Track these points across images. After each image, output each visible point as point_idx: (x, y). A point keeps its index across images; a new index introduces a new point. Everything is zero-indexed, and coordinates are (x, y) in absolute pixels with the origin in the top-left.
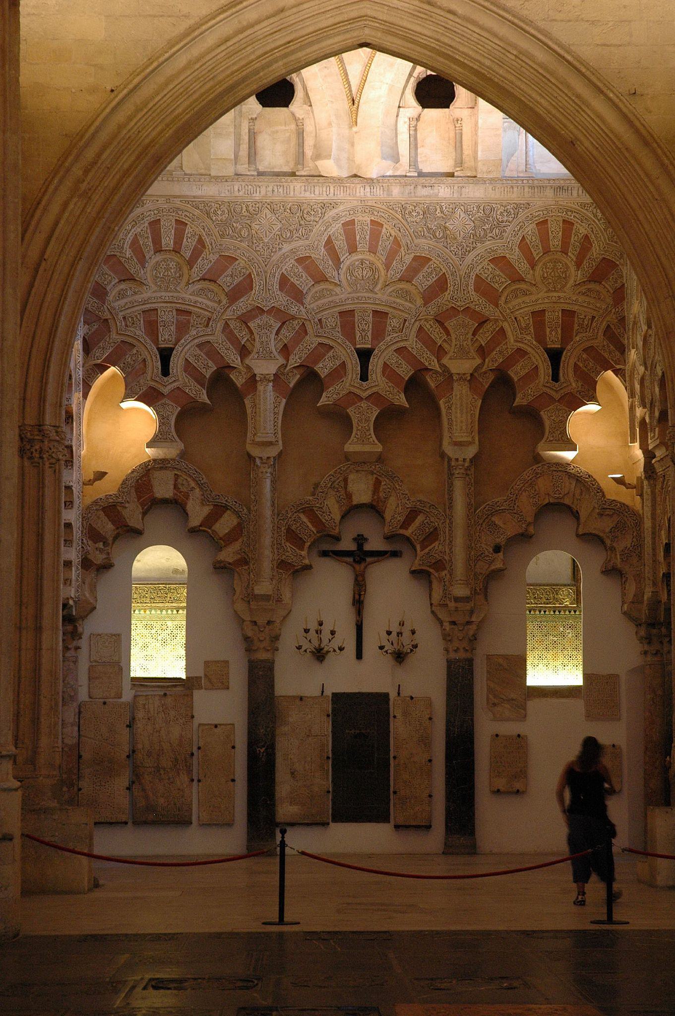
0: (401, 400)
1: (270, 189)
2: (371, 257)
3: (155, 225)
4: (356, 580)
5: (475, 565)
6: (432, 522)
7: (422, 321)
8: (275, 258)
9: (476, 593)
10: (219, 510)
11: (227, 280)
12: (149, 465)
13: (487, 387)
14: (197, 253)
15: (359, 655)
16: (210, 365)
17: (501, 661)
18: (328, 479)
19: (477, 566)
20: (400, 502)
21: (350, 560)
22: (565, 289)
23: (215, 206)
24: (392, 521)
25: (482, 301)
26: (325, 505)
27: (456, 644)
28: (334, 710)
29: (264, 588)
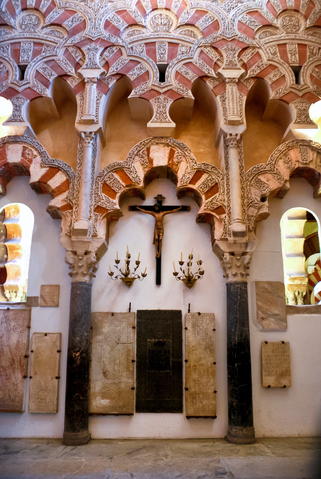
2: (167, 13)
4: (156, 225)
5: (248, 210)
6: (213, 179)
8: (101, 11)
9: (250, 231)
12: (5, 140)
13: (250, 88)
14: (49, 10)
15: (158, 282)
16: (53, 73)
17: (266, 286)
19: (249, 211)
20: (189, 165)
22: (299, 32)
24: (184, 178)
27: (234, 271)
28: (138, 323)
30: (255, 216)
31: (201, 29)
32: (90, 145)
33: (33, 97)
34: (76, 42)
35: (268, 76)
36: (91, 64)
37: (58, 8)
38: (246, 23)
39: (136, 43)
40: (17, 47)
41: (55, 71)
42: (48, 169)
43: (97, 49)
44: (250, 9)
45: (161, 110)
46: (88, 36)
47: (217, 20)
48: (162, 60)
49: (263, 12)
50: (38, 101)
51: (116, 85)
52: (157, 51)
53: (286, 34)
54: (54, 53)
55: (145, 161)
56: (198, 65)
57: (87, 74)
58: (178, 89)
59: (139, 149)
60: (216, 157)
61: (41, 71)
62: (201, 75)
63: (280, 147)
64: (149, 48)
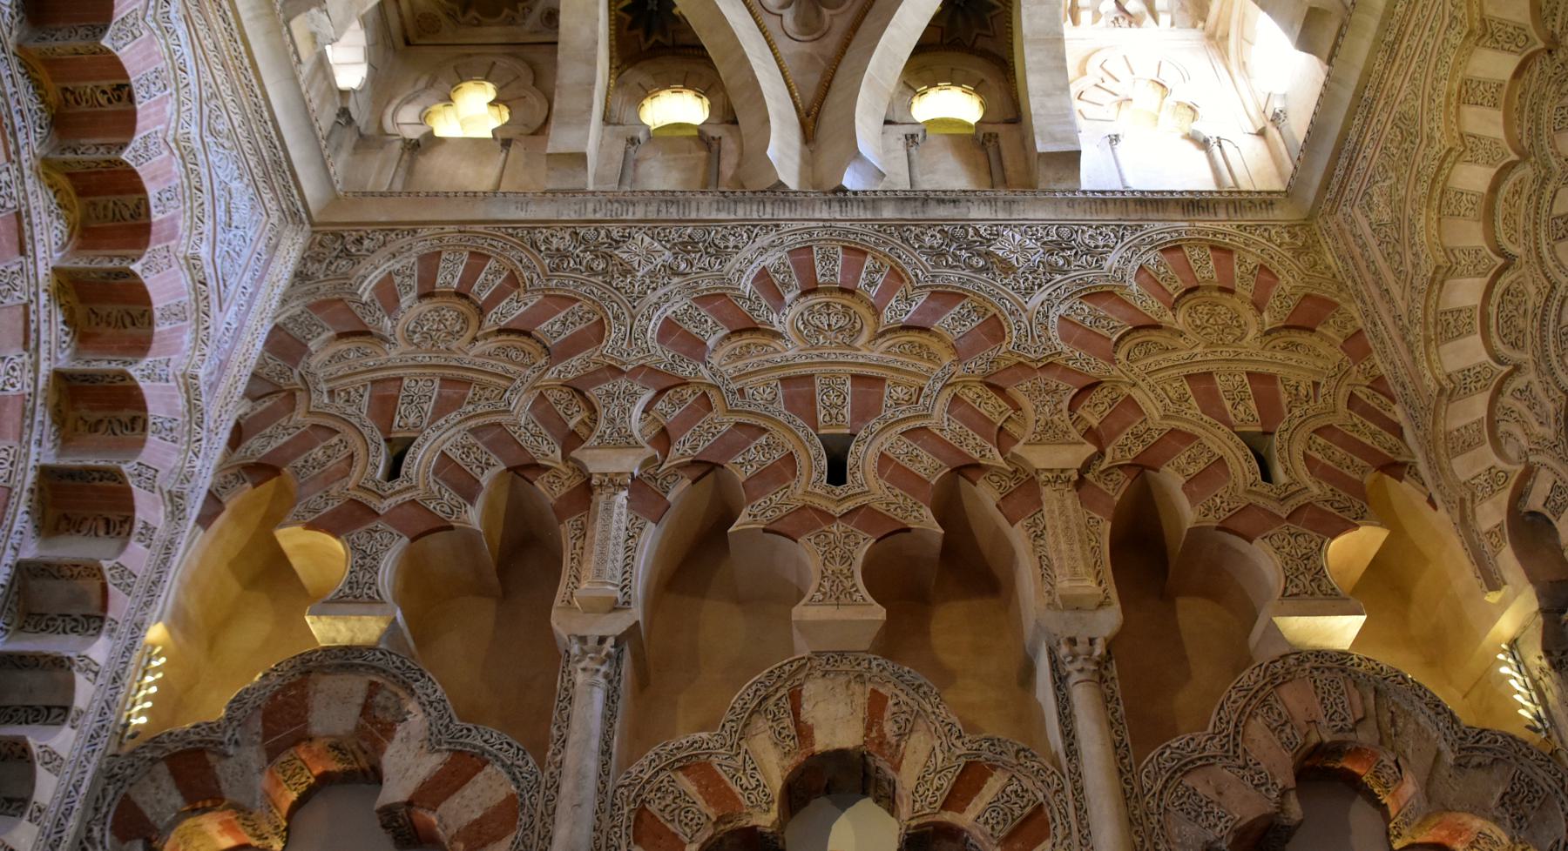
2: (846, 300)
3: (430, 262)
7: (959, 388)
8: (652, 297)
11: (552, 328)
12: (311, 660)
13: (1117, 498)
20: (937, 743)
22: (1244, 343)
24: (921, 790)
26: (742, 752)
31: (950, 339)
33: (423, 528)
34: (570, 376)
35: (1170, 462)
37: (526, 292)
40: (391, 390)
42: (446, 755)
43: (635, 393)
44: (1090, 288)
45: (837, 567)
46: (608, 361)
50: (436, 542)
52: (818, 398)
54: (502, 405)
55: (785, 732)
57: (600, 461)
58: (888, 504)
59: (763, 692)
60: (1027, 716)
61: (455, 455)
62: (959, 462)
63: (1246, 678)
64: (794, 389)
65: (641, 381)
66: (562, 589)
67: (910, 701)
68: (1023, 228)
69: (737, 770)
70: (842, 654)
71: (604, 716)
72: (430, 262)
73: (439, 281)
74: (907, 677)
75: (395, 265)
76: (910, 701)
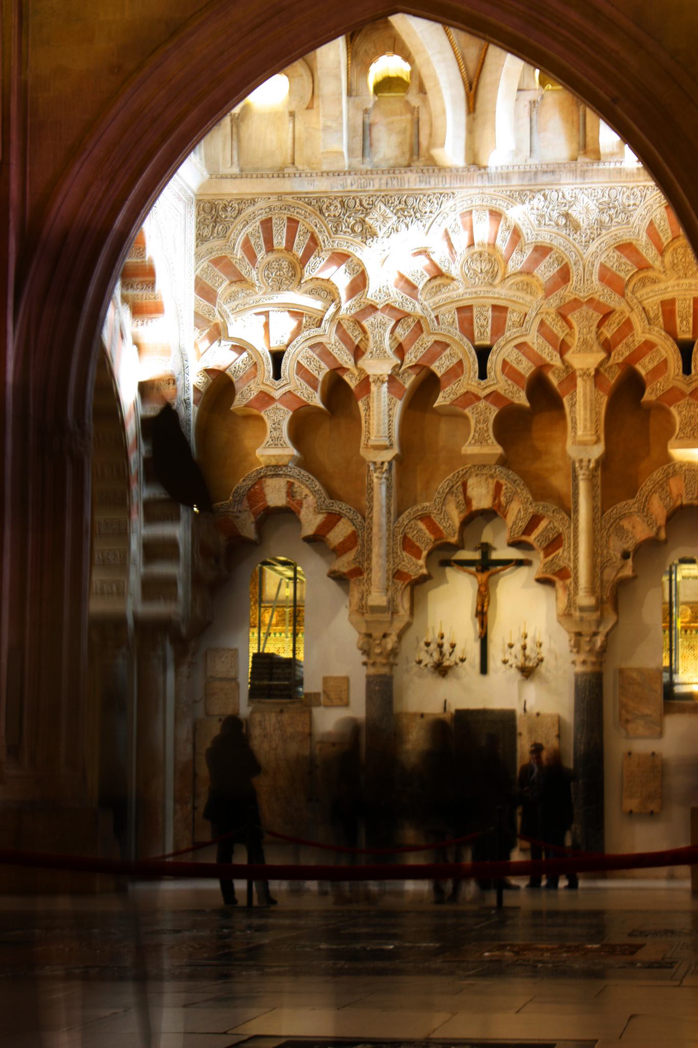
0: (521, 399)
1: (384, 181)
3: (267, 224)
10: (332, 519)
13: (613, 382)
15: (484, 669)
16: (322, 367)
17: (634, 675)
18: (446, 484)
20: (522, 507)
21: (473, 569)
23: (327, 201)
25: (607, 290)
29: (377, 598)
30: (612, 581)
32: (384, 480)
36: (378, 351)
38: (612, 267)
39: (443, 309)
41: (326, 363)
42: (325, 515)
45: (481, 426)
47: (566, 263)
48: (482, 337)
49: (641, 245)
51: (414, 384)
53: (677, 279)
56: (535, 347)
59: (451, 484)
61: (304, 363)
65: (388, 315)
66: (363, 438)
67: (512, 487)
68: (590, 190)
69: (441, 519)
70: (484, 466)
71: (387, 497)
72: (267, 224)
73: (275, 242)
74: (511, 476)
75: (249, 229)
76: (512, 487)
